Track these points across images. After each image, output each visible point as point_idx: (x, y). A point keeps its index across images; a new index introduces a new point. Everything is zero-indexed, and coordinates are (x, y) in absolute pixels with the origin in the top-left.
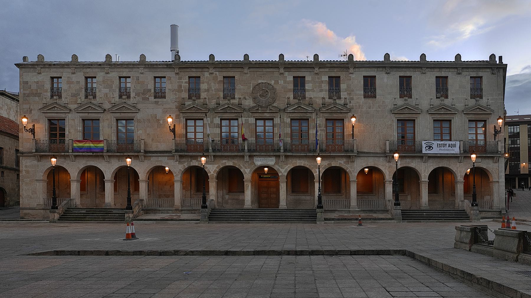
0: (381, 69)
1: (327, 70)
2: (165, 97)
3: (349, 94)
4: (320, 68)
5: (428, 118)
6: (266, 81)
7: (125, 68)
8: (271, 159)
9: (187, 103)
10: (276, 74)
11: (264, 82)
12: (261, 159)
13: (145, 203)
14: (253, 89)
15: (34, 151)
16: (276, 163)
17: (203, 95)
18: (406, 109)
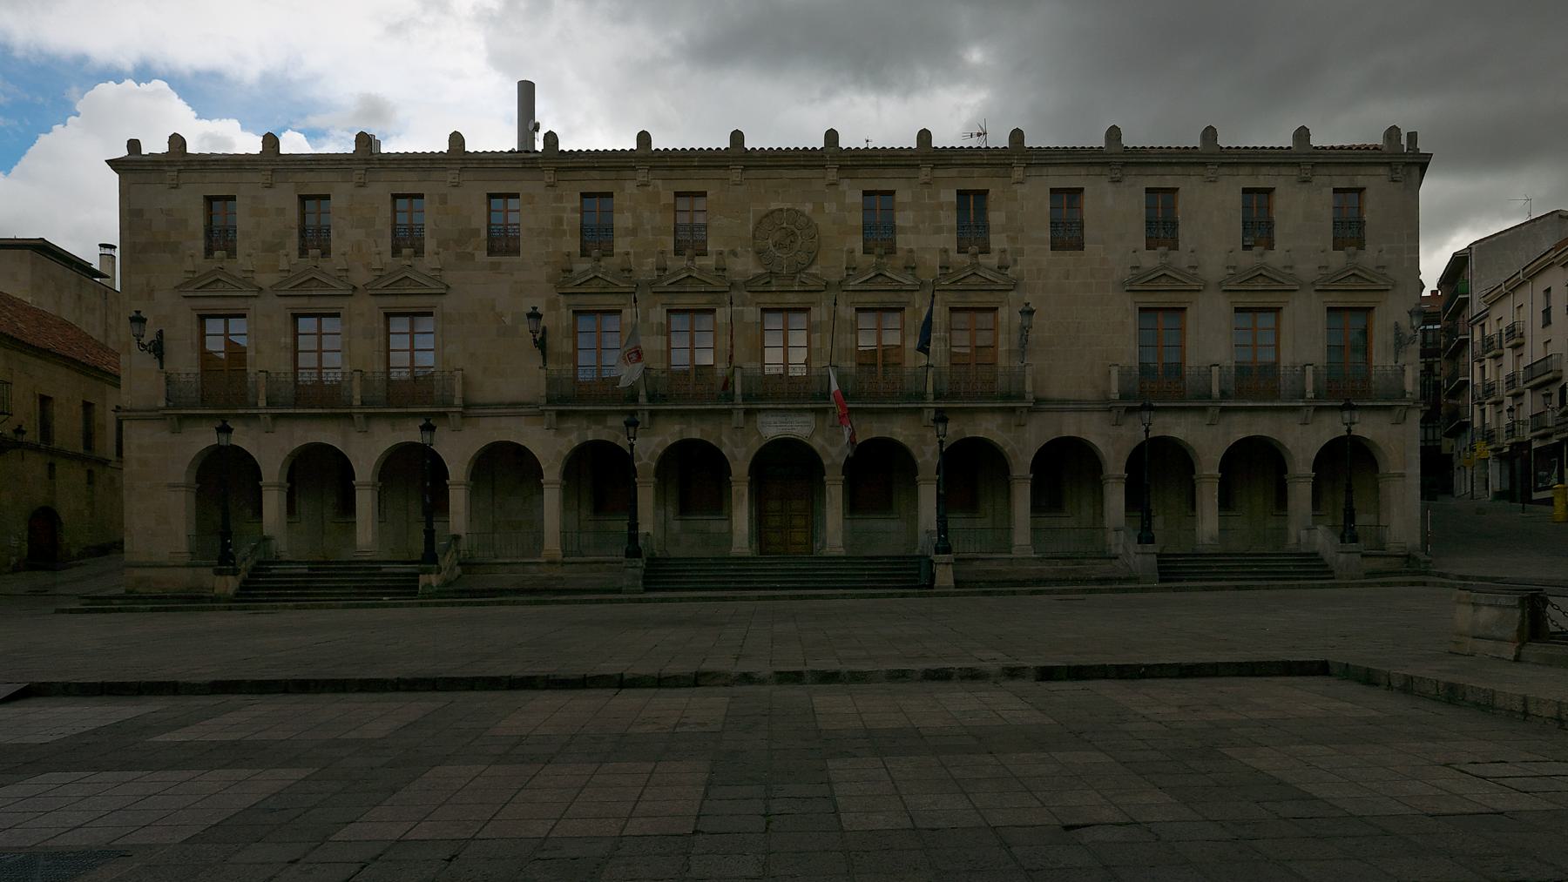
0: (1098, 170)
1: (953, 172)
2: (517, 252)
4: (935, 167)
6: (789, 205)
7: (410, 170)
13: (463, 545)
14: (756, 229)
15: (162, 403)
17: (621, 245)
18: (1164, 280)
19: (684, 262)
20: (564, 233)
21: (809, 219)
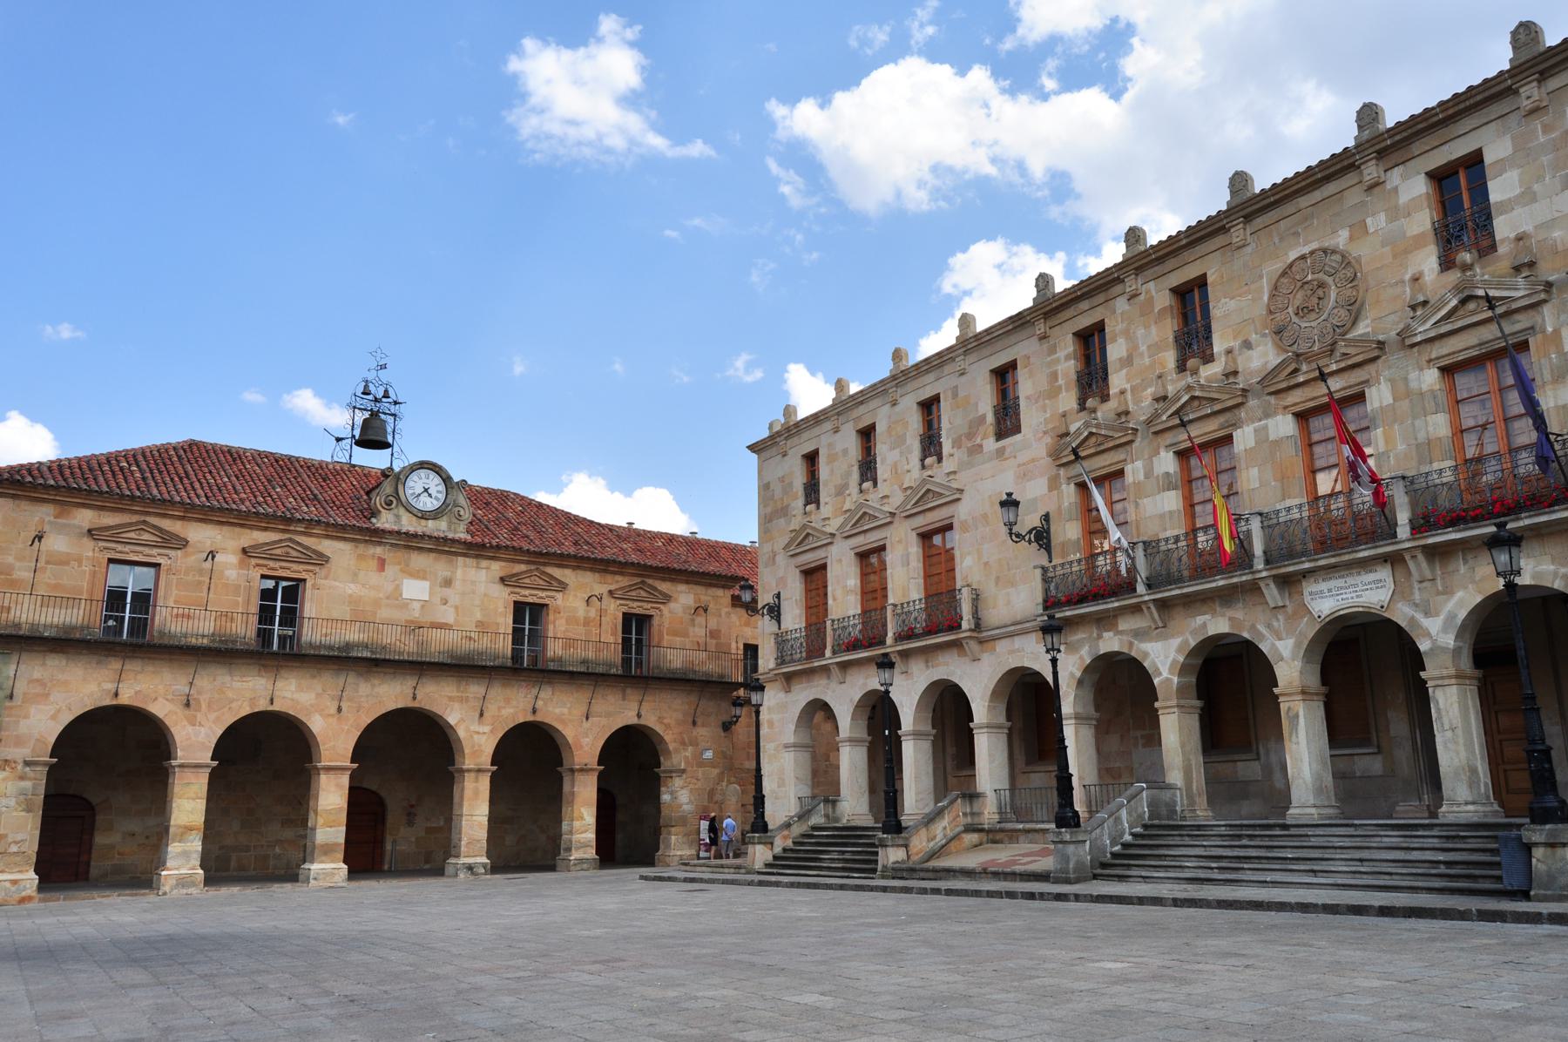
6: (1314, 246)
7: (927, 371)
8: (1371, 577)
9: (1073, 428)
10: (1354, 197)
11: (1306, 250)
12: (1333, 583)
14: (1272, 296)
16: (1399, 593)
17: (1117, 381)
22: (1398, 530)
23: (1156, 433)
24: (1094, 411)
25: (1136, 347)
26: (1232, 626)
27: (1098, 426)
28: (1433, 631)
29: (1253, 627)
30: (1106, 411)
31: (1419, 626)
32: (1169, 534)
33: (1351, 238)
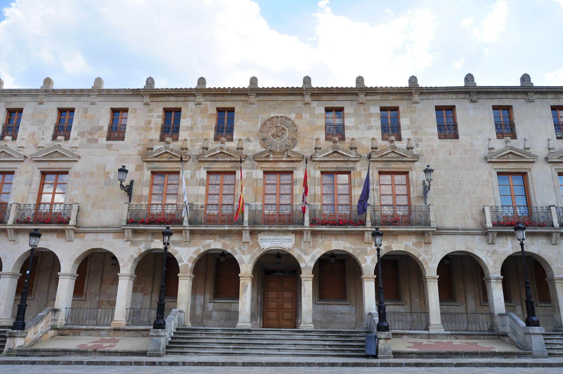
0: (463, 96)
1: (378, 97)
2: (123, 139)
3: (415, 133)
5: (549, 171)
6: (282, 115)
7: (69, 95)
9: (156, 147)
10: (299, 104)
11: (278, 115)
12: (271, 237)
16: (297, 245)
17: (183, 134)
19: (218, 145)
20: (151, 128)
21: (293, 123)
22: (305, 223)
23: (200, 161)
24: (168, 143)
25: (196, 124)
26: (223, 247)
27: (172, 150)
28: (307, 261)
29: (233, 248)
30: (175, 146)
31: (302, 258)
32: (199, 203)
33: (296, 117)
